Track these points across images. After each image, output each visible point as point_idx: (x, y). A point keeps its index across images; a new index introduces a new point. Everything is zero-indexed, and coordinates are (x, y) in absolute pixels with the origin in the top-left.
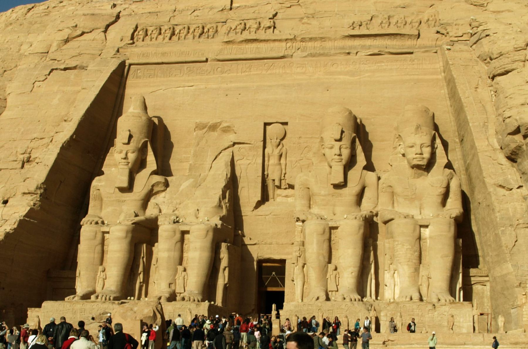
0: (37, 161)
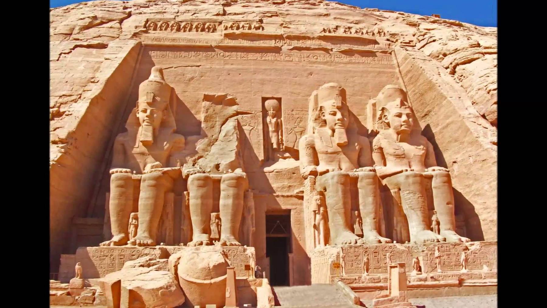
0: (66, 113)
